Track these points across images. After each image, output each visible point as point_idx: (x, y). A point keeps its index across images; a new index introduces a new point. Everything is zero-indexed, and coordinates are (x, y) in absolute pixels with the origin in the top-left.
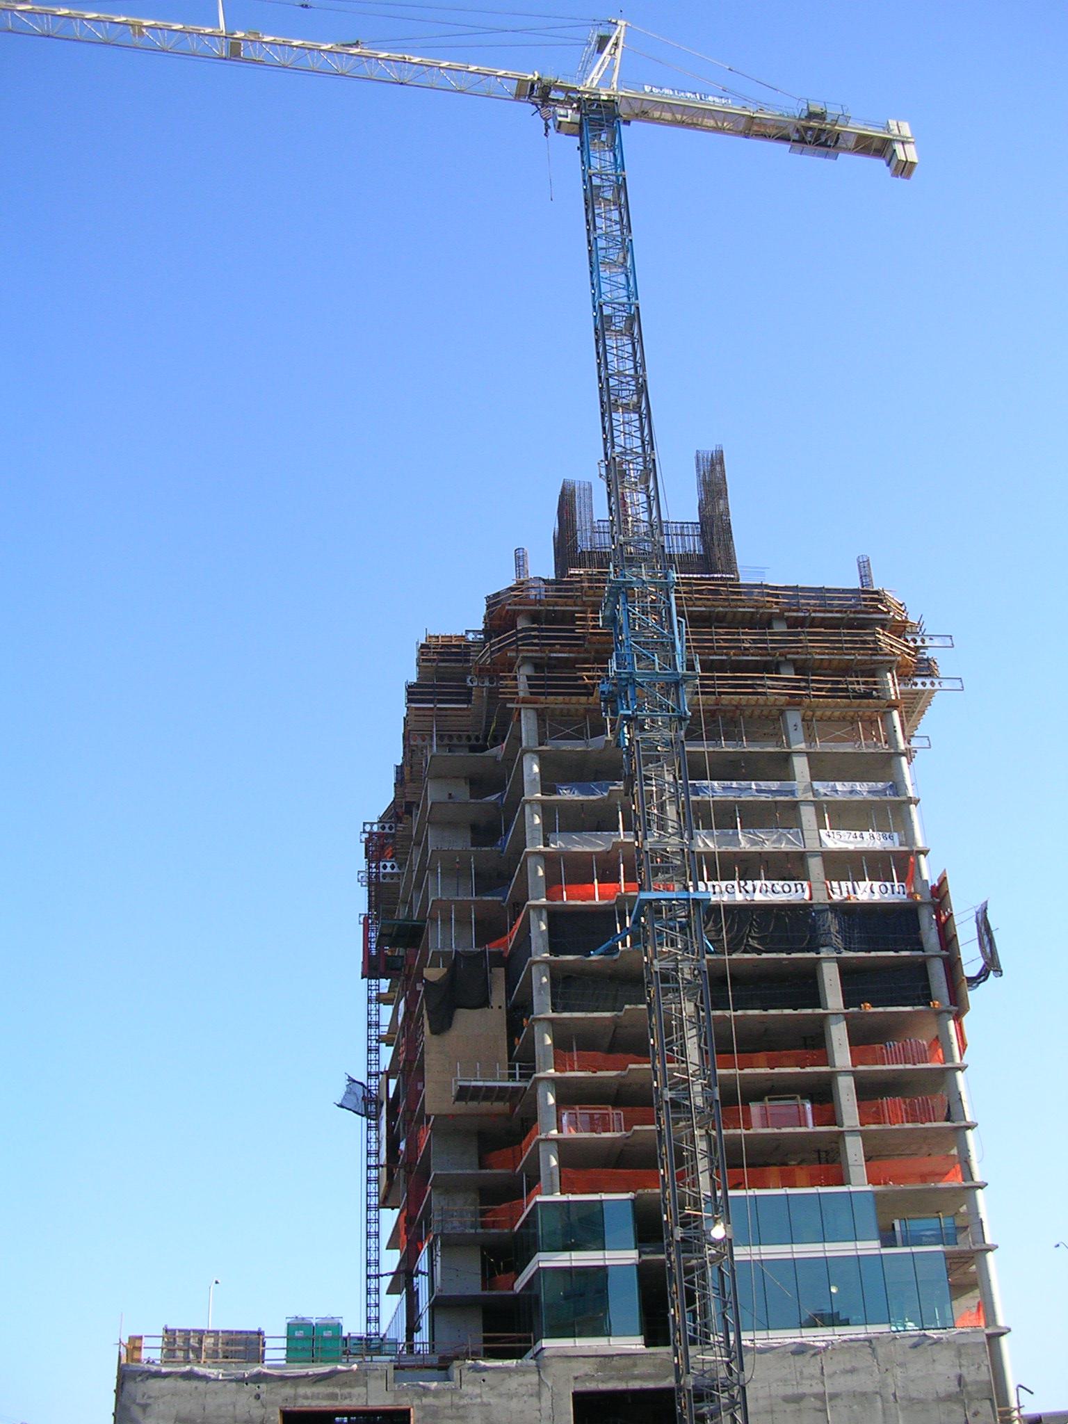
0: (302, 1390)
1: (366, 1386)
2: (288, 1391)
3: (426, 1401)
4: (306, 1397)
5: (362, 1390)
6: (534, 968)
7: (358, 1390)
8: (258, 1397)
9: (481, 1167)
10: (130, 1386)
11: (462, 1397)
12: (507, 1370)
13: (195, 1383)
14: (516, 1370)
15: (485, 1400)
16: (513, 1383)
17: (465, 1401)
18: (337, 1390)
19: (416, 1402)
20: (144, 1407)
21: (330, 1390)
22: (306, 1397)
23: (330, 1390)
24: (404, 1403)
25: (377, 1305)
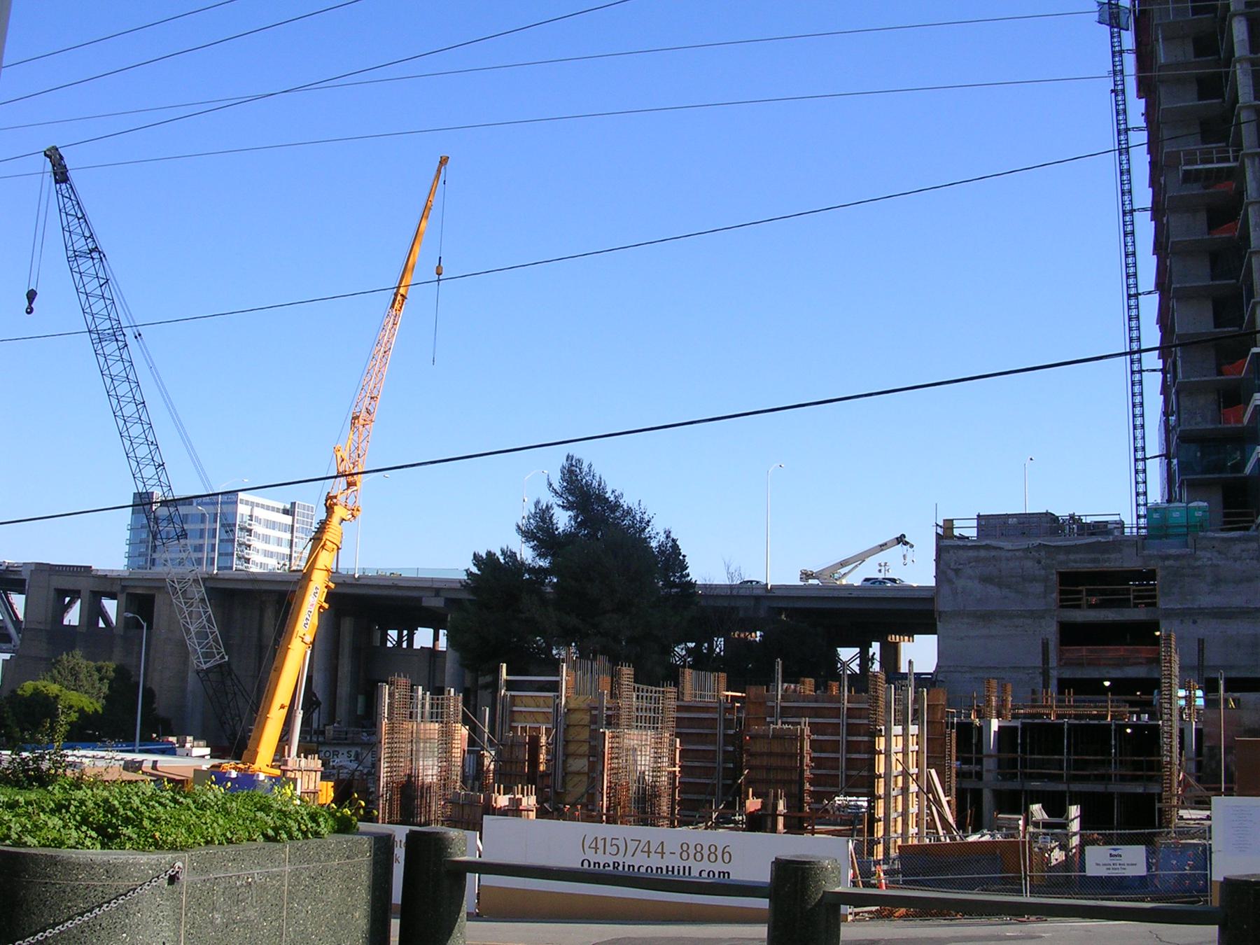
0: (1072, 557)
1: (1120, 551)
2: (1062, 557)
3: (1167, 563)
4: (1075, 562)
5: (1119, 555)
6: (1250, 209)
7: (1113, 556)
8: (1039, 562)
9: (1220, 373)
10: (945, 556)
11: (1196, 559)
12: (1231, 539)
13: (993, 553)
14: (1239, 539)
15: (1215, 562)
16: (1237, 549)
17: (1199, 563)
18: (1099, 556)
19: (1161, 564)
20: (957, 571)
21: (1093, 556)
22: (1075, 562)
23: (1093, 556)
24: (1152, 565)
25: (1145, 482)
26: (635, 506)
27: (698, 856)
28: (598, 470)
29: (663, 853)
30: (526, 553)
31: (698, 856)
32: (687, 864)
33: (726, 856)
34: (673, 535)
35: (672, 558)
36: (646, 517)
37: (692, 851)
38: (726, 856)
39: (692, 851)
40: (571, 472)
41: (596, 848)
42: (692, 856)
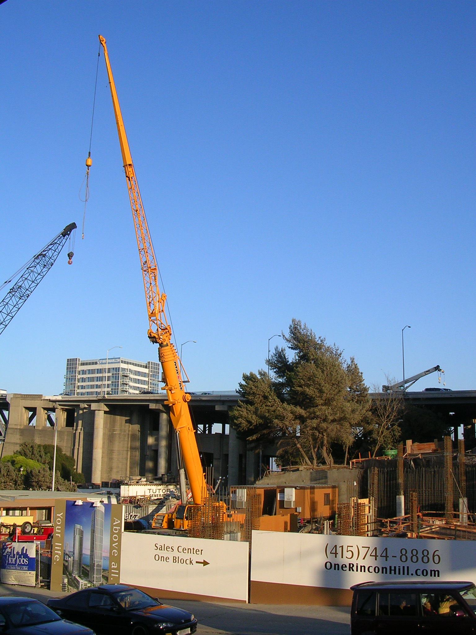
26: (332, 346)
27: (415, 559)
28: (309, 327)
29: (386, 557)
30: (272, 375)
31: (415, 559)
32: (406, 565)
33: (436, 558)
34: (356, 362)
35: (354, 373)
36: (339, 352)
37: (409, 555)
38: (436, 558)
39: (409, 555)
40: (296, 328)
41: (336, 554)
42: (409, 559)
